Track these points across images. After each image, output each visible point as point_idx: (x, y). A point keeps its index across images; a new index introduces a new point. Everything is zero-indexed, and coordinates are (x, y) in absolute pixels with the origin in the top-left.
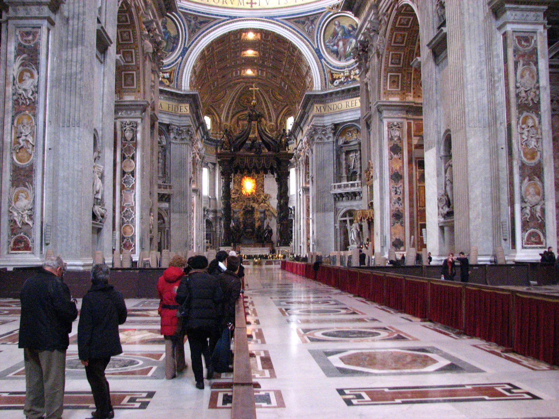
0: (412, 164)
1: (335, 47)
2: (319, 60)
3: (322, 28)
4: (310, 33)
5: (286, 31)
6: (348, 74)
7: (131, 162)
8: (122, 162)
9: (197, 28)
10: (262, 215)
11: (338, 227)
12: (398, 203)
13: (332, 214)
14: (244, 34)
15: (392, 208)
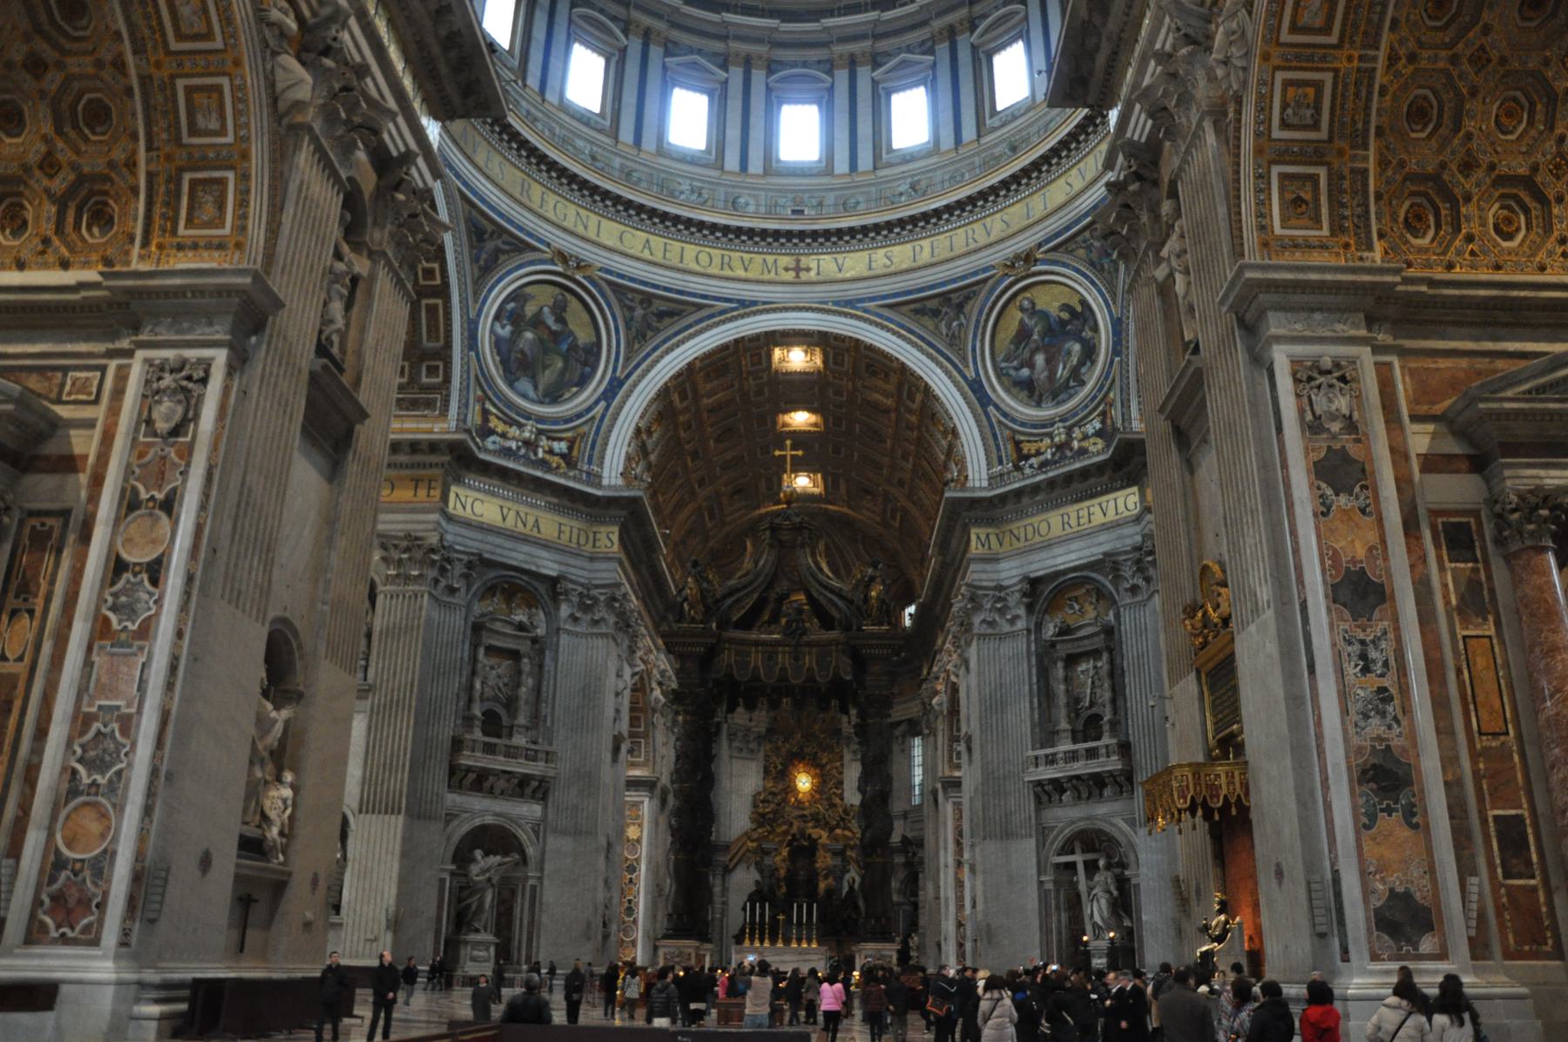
0: (1419, 538)
1: (1025, 372)
2: (980, 410)
3: (987, 320)
4: (954, 340)
5: (889, 335)
6: (1063, 436)
7: (158, 519)
8: (117, 522)
9: (649, 327)
10: (838, 861)
11: (1050, 886)
12: (1383, 714)
13: (1031, 844)
14: (777, 353)
15: (1356, 741)
